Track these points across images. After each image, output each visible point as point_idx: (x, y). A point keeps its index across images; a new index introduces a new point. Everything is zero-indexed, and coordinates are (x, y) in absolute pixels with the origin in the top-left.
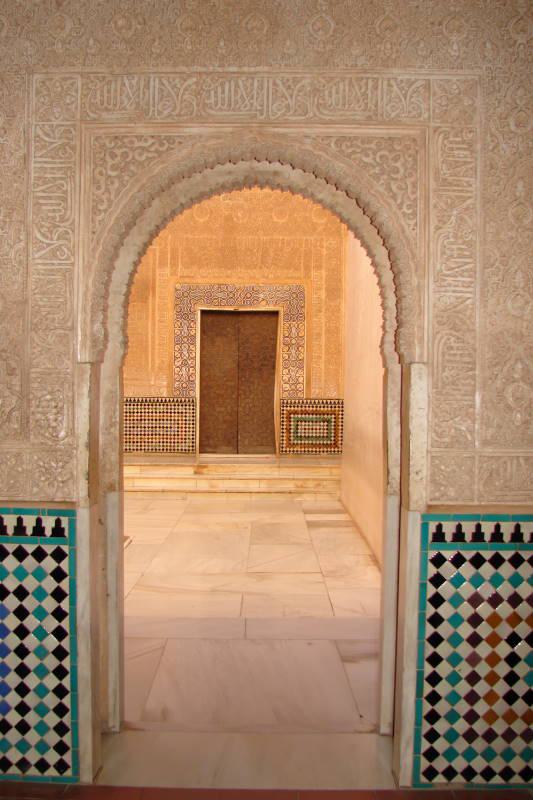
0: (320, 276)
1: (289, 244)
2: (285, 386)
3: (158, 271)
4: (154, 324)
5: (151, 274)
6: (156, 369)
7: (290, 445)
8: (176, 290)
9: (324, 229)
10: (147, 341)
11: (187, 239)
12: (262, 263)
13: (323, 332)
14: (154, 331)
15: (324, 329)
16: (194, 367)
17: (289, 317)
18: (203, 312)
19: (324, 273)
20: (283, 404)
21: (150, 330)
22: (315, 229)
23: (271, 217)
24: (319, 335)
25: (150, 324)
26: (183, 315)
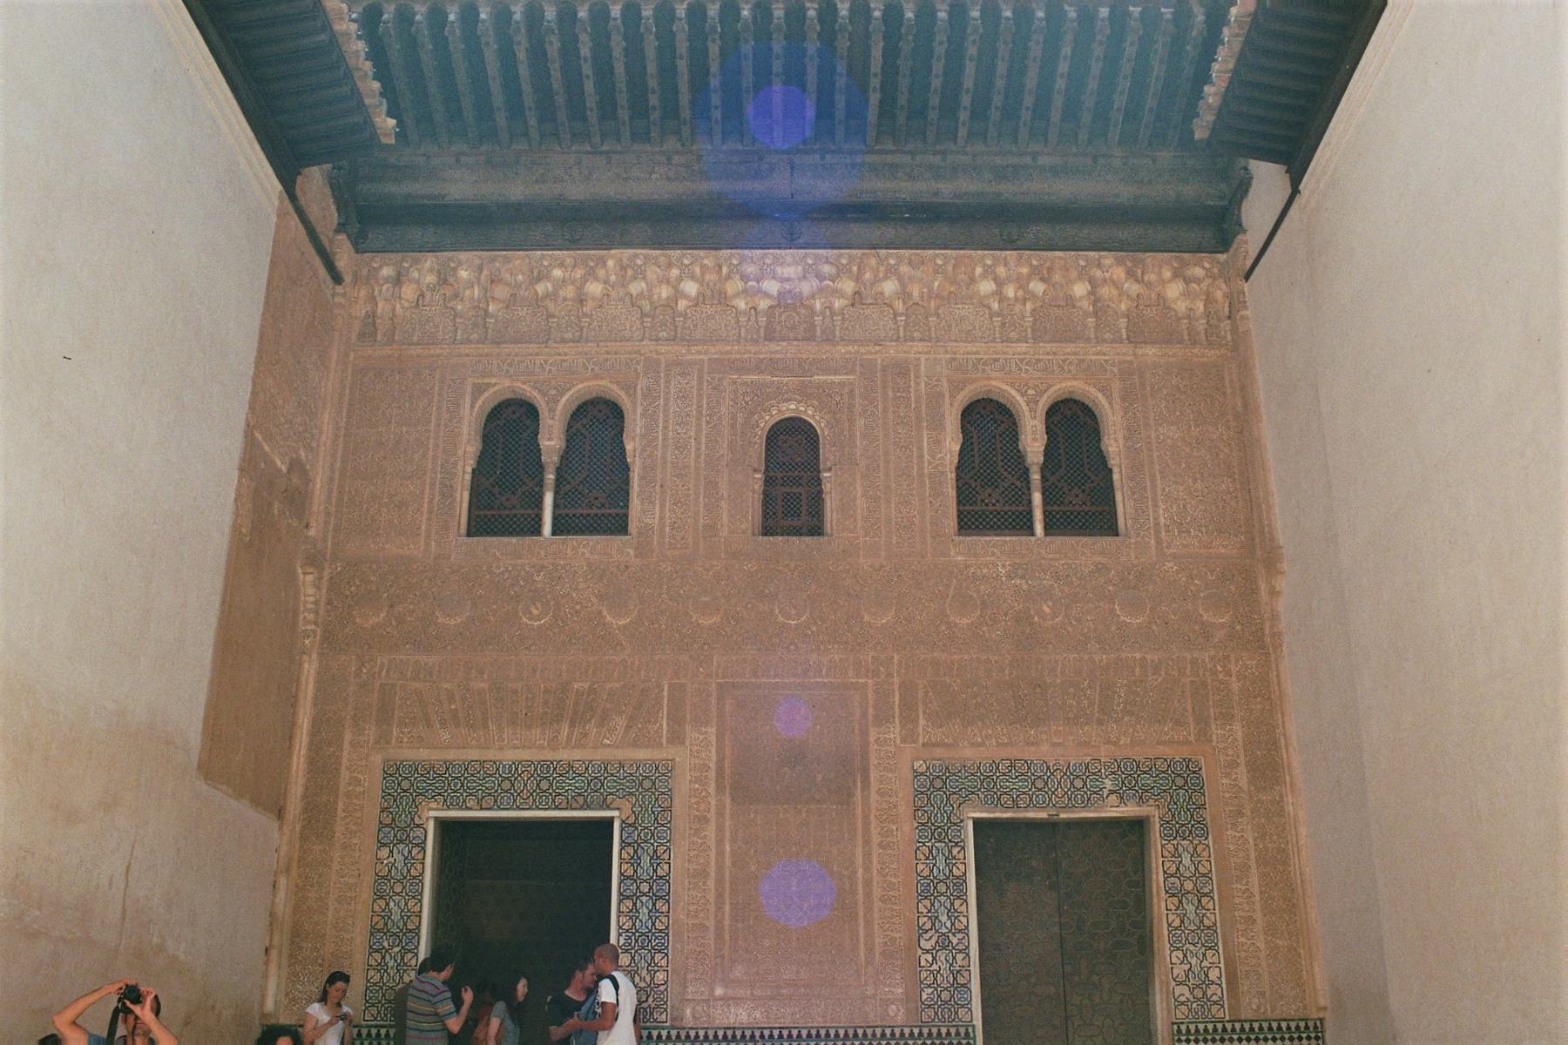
1: (1156, 670)
2: (1179, 989)
3: (873, 735)
4: (867, 855)
8: (916, 774)
10: (854, 892)
13: (1254, 866)
14: (867, 869)
15: (1253, 855)
16: (966, 951)
17: (1175, 830)
18: (978, 823)
19: (1238, 730)
21: (859, 859)
23: (1112, 611)
24: (1244, 869)
25: (859, 851)
26: (937, 830)
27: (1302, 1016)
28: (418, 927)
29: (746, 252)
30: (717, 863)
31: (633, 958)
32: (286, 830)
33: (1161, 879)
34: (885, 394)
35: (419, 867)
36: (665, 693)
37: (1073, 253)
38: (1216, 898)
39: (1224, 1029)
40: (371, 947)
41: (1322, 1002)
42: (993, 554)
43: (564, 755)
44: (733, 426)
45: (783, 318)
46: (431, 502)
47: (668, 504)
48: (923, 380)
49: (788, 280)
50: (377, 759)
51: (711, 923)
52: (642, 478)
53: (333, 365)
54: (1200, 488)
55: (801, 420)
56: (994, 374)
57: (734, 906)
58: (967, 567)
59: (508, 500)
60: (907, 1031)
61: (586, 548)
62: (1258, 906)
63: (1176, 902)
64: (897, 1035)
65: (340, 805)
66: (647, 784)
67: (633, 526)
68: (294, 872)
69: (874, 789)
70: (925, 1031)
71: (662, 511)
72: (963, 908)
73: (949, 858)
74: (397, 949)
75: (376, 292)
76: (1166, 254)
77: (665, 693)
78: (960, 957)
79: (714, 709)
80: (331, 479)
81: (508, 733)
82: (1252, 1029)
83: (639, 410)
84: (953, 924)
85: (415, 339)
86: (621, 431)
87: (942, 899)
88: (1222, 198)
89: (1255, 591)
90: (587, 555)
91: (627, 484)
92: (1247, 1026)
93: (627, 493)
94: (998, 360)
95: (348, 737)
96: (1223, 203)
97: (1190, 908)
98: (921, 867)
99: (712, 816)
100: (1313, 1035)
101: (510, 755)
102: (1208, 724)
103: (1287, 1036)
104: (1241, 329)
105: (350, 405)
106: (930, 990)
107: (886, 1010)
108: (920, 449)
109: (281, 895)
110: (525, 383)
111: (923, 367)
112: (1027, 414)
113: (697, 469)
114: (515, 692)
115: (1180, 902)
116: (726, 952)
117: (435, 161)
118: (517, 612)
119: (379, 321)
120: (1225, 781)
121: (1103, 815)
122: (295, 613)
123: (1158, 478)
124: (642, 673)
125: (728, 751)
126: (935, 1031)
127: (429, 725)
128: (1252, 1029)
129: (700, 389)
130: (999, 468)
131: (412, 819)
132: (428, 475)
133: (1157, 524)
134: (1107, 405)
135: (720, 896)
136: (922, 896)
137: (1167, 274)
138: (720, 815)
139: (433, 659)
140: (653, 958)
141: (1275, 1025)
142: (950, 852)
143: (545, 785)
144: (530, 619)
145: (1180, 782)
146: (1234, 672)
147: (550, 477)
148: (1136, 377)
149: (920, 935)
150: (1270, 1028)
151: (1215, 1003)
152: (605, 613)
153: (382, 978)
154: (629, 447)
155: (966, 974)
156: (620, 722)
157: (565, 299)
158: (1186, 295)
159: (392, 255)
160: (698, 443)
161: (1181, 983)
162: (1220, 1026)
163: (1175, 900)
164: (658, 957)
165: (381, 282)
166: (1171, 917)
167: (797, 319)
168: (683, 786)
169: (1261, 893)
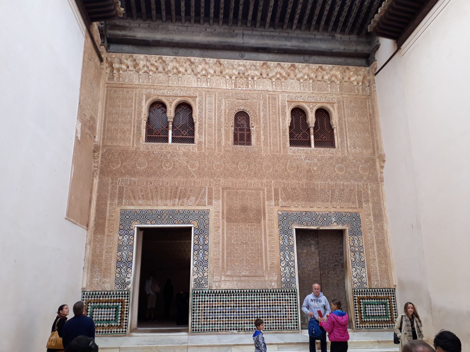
0: (368, 207)
2: (355, 279)
3: (266, 203)
4: (265, 238)
5: (262, 205)
6: (269, 269)
7: (362, 322)
9: (368, 178)
10: (262, 249)
11: (284, 183)
12: (332, 198)
14: (265, 242)
15: (375, 241)
18: (297, 230)
19: (371, 205)
20: (354, 292)
21: (263, 240)
22: (362, 178)
23: (334, 170)
24: (373, 244)
26: (284, 231)
27: (389, 287)
28: (132, 260)
29: (229, 60)
30: (222, 240)
31: (198, 269)
32: (89, 231)
33: (349, 247)
34: (269, 105)
35: (132, 242)
36: (207, 190)
37: (325, 65)
38: (364, 253)
39: (367, 291)
40: (117, 267)
41: (395, 284)
42: (300, 153)
43: (176, 208)
44: (225, 113)
45: (239, 81)
46: (134, 131)
47: (207, 135)
48: (280, 101)
49: (241, 70)
50: (118, 209)
51: (221, 258)
52: (199, 127)
53: (101, 87)
54: (359, 135)
55: (244, 112)
56: (301, 101)
57: (227, 253)
58: (293, 156)
59: (157, 132)
60: (277, 290)
61: (183, 147)
62: (376, 256)
63: (353, 254)
64: (275, 292)
65: (107, 223)
66: (202, 217)
67: (196, 140)
68: (92, 245)
69: (267, 218)
70: (283, 290)
71: (205, 137)
72: (293, 254)
73: (289, 240)
74: (125, 267)
75: (114, 66)
76: (352, 67)
77: (207, 190)
78: (292, 268)
79: (221, 195)
80: (102, 123)
81: (159, 201)
82: (375, 291)
83: (197, 107)
84: (290, 259)
85: (126, 81)
86: (192, 113)
87: (287, 251)
88: (369, 50)
89: (375, 165)
90: (183, 149)
91: (194, 129)
92: (373, 290)
93: (194, 131)
94: (301, 96)
95: (109, 202)
96: (369, 52)
97: (357, 256)
98: (281, 242)
99: (221, 226)
100: (392, 293)
101: (160, 208)
102: (362, 203)
103: (385, 293)
104: (373, 90)
105: (106, 100)
106: (284, 278)
107: (271, 284)
108: (279, 122)
109: (88, 251)
110: (162, 96)
111: (280, 98)
112: (310, 113)
113: (215, 126)
114: (162, 189)
115: (355, 254)
116: (225, 266)
117: (132, 25)
118: (161, 166)
119: (114, 75)
120: (367, 219)
121: (332, 228)
122: (91, 165)
123: (348, 132)
124: (200, 184)
125: (225, 207)
126: (285, 290)
127: (135, 198)
128: (375, 291)
129: (215, 102)
130: (301, 128)
131: (130, 227)
132: (133, 123)
133: (347, 145)
134: (333, 111)
135: (223, 250)
136: (281, 250)
137: (352, 73)
138: (223, 226)
139: (137, 179)
140: (203, 268)
141: (381, 290)
142: (289, 238)
143: (171, 217)
144: (166, 168)
145: (354, 219)
146: (369, 189)
147: (171, 126)
148: (342, 102)
149: (281, 262)
150: (380, 291)
151: (365, 283)
152: (189, 166)
153: (120, 276)
154: (194, 118)
155: (294, 274)
156: (193, 198)
157: (173, 72)
158: (355, 80)
159: (118, 54)
160: (215, 118)
161: (355, 277)
162: (366, 290)
163: (353, 253)
164: (205, 268)
165: (115, 62)
166: (352, 258)
167: (243, 81)
168: (212, 217)
169: (377, 252)
